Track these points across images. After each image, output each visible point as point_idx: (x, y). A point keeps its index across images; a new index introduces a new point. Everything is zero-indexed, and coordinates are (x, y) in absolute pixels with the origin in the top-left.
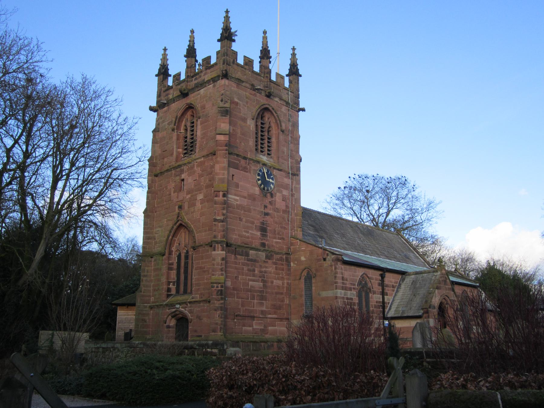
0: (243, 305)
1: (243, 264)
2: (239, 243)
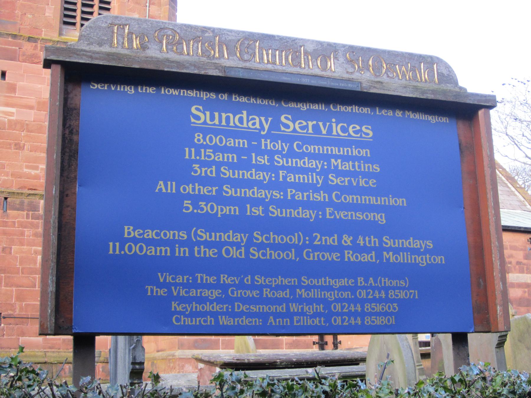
0: (19, 298)
1: (22, 225)
2: (14, 190)
